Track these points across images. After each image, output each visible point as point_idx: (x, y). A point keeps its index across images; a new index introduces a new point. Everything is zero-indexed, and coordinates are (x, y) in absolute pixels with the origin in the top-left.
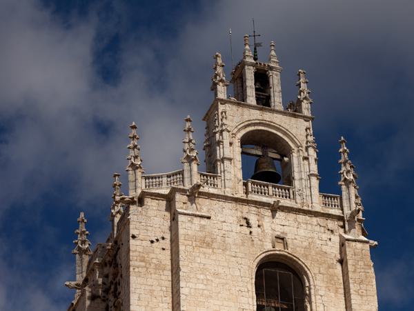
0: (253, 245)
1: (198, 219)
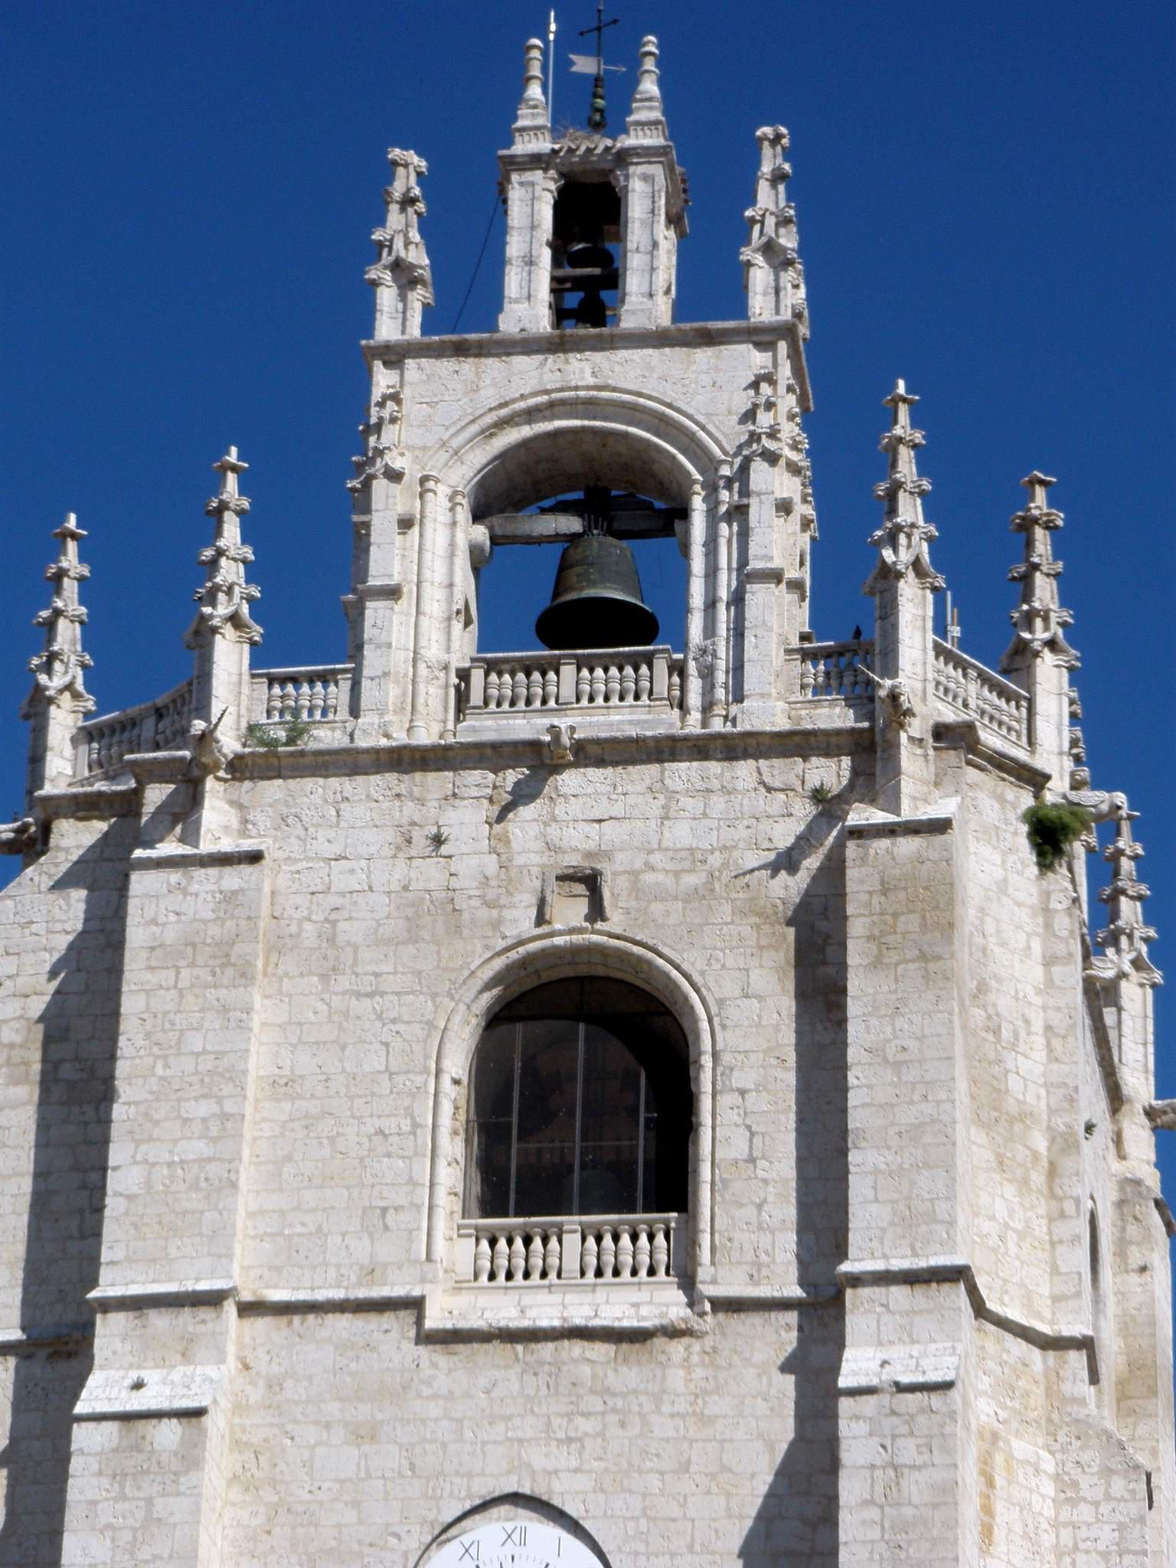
0: (458, 929)
1: (213, 872)
